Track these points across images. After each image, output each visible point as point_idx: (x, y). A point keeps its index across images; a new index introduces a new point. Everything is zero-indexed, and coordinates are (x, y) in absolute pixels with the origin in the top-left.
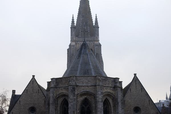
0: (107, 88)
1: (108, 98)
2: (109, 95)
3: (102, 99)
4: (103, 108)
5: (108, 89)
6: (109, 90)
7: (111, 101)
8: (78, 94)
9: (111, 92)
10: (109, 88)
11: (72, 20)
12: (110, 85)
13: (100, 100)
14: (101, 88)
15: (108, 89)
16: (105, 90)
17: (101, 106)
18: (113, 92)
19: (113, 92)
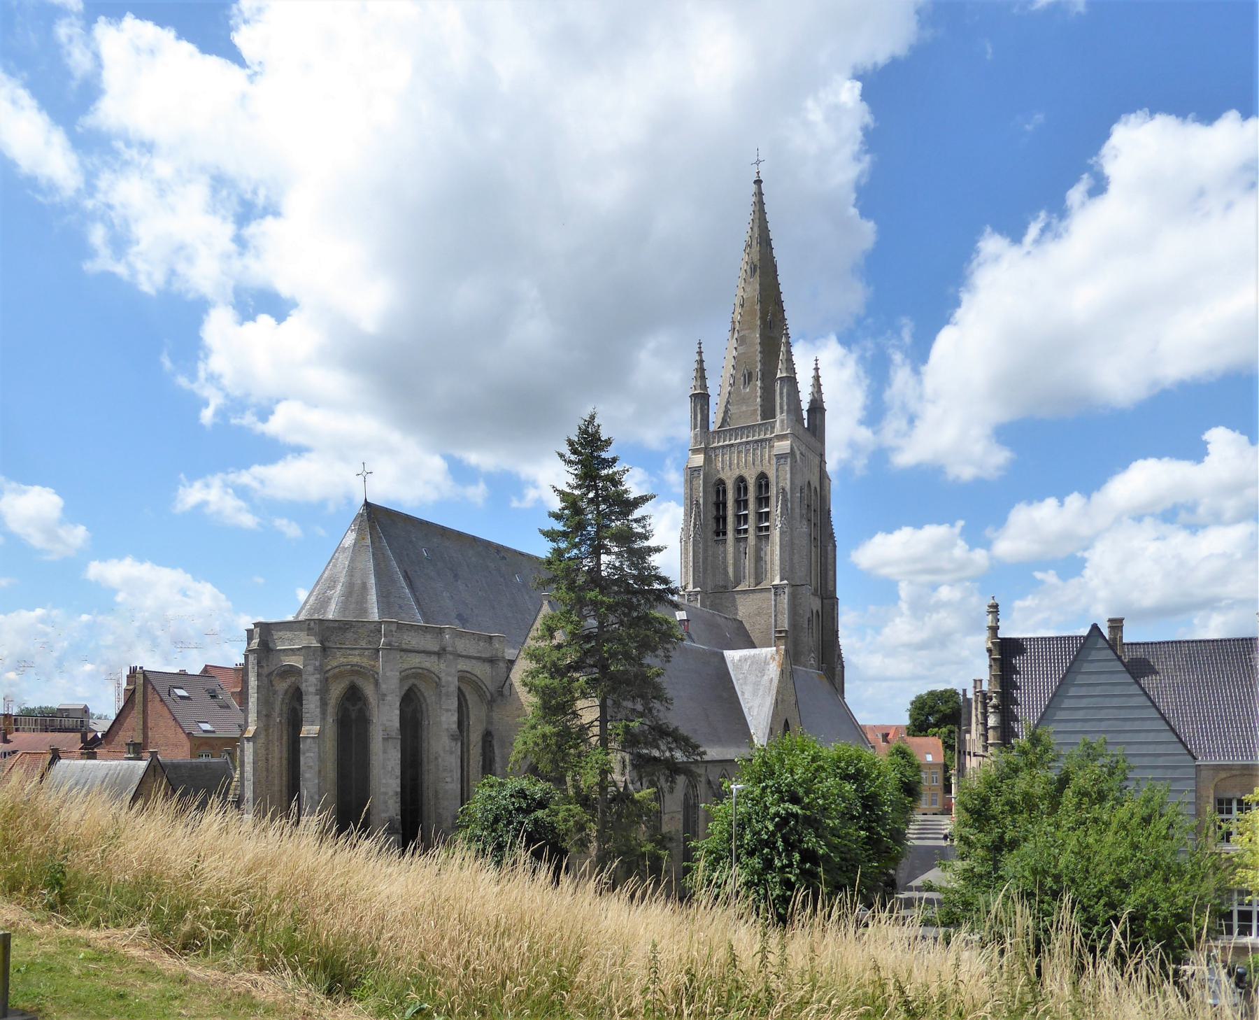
0: (349, 652)
1: (360, 682)
2: (357, 671)
3: (316, 685)
4: (318, 710)
5: (355, 655)
6: (356, 660)
7: (369, 690)
8: (270, 674)
9: (365, 662)
10: (357, 652)
11: (696, 366)
12: (363, 644)
13: (312, 689)
14: (314, 655)
15: (355, 655)
16: (337, 660)
17: (312, 706)
18: (373, 663)
19: (373, 663)
